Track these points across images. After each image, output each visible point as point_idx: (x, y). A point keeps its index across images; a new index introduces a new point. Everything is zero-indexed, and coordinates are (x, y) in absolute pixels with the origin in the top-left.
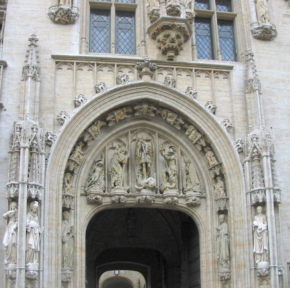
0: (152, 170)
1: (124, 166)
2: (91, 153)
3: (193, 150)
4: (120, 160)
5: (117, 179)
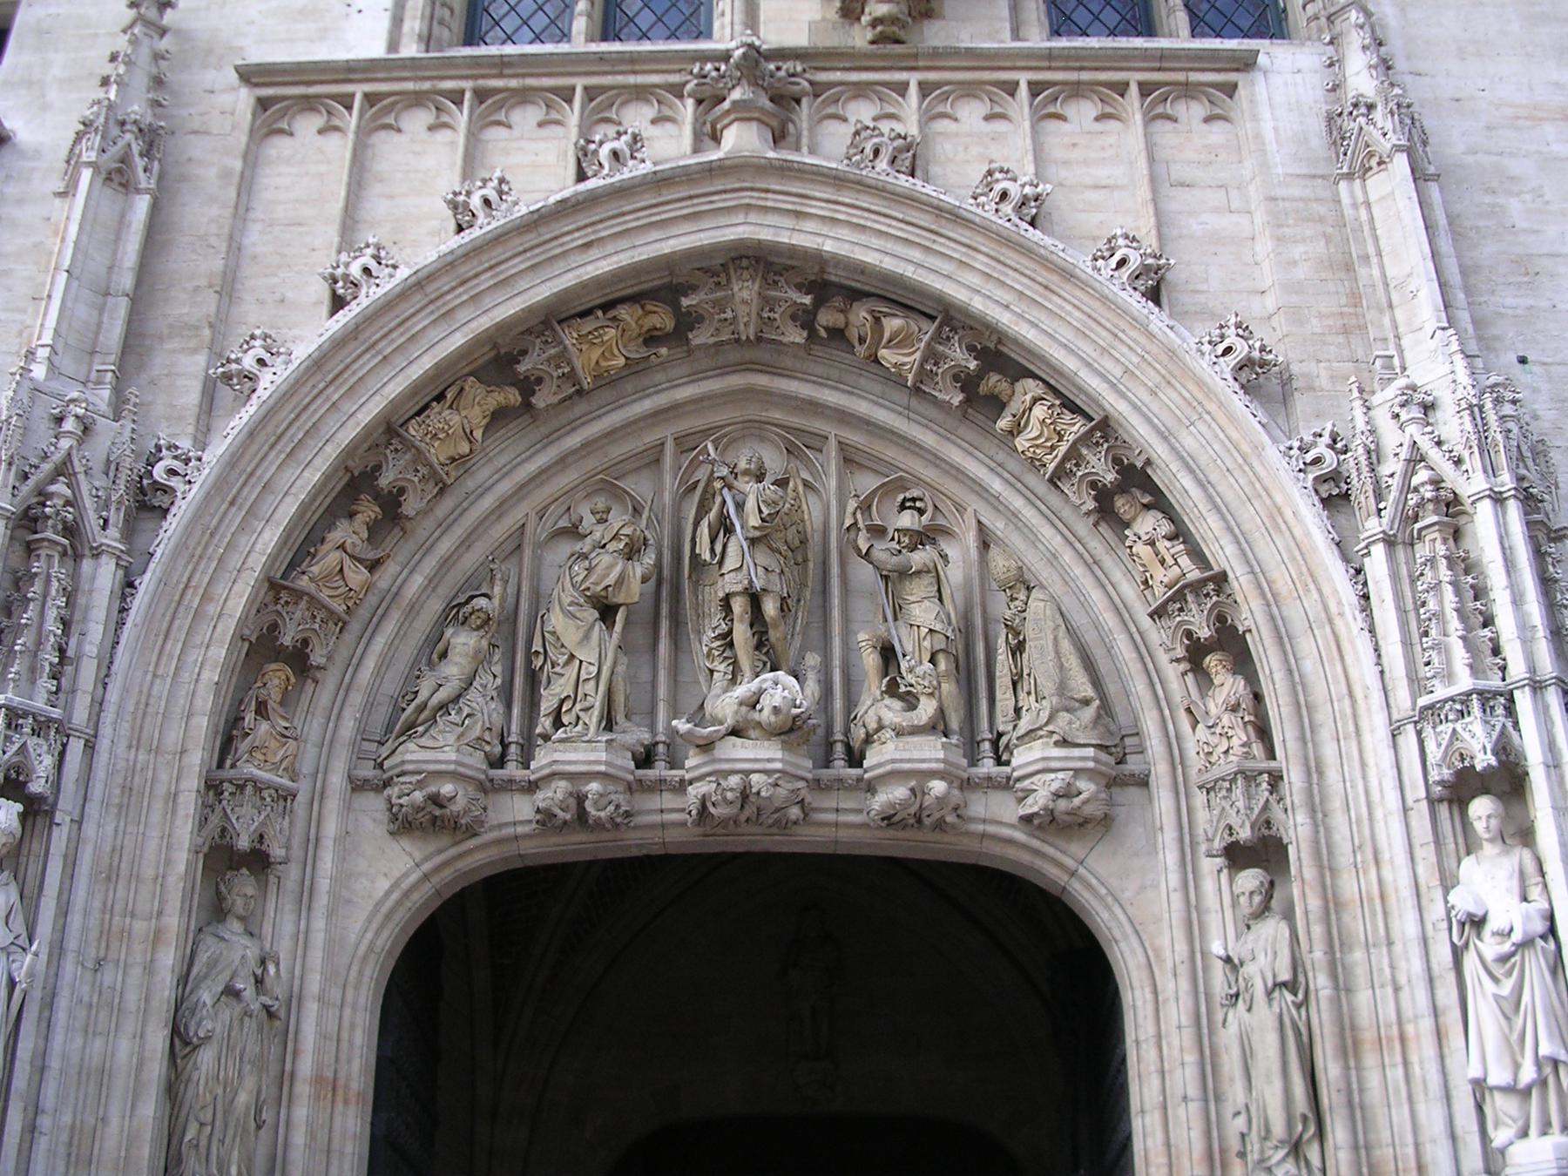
1: (620, 617)
2: (428, 558)
4: (596, 584)
5: (569, 691)
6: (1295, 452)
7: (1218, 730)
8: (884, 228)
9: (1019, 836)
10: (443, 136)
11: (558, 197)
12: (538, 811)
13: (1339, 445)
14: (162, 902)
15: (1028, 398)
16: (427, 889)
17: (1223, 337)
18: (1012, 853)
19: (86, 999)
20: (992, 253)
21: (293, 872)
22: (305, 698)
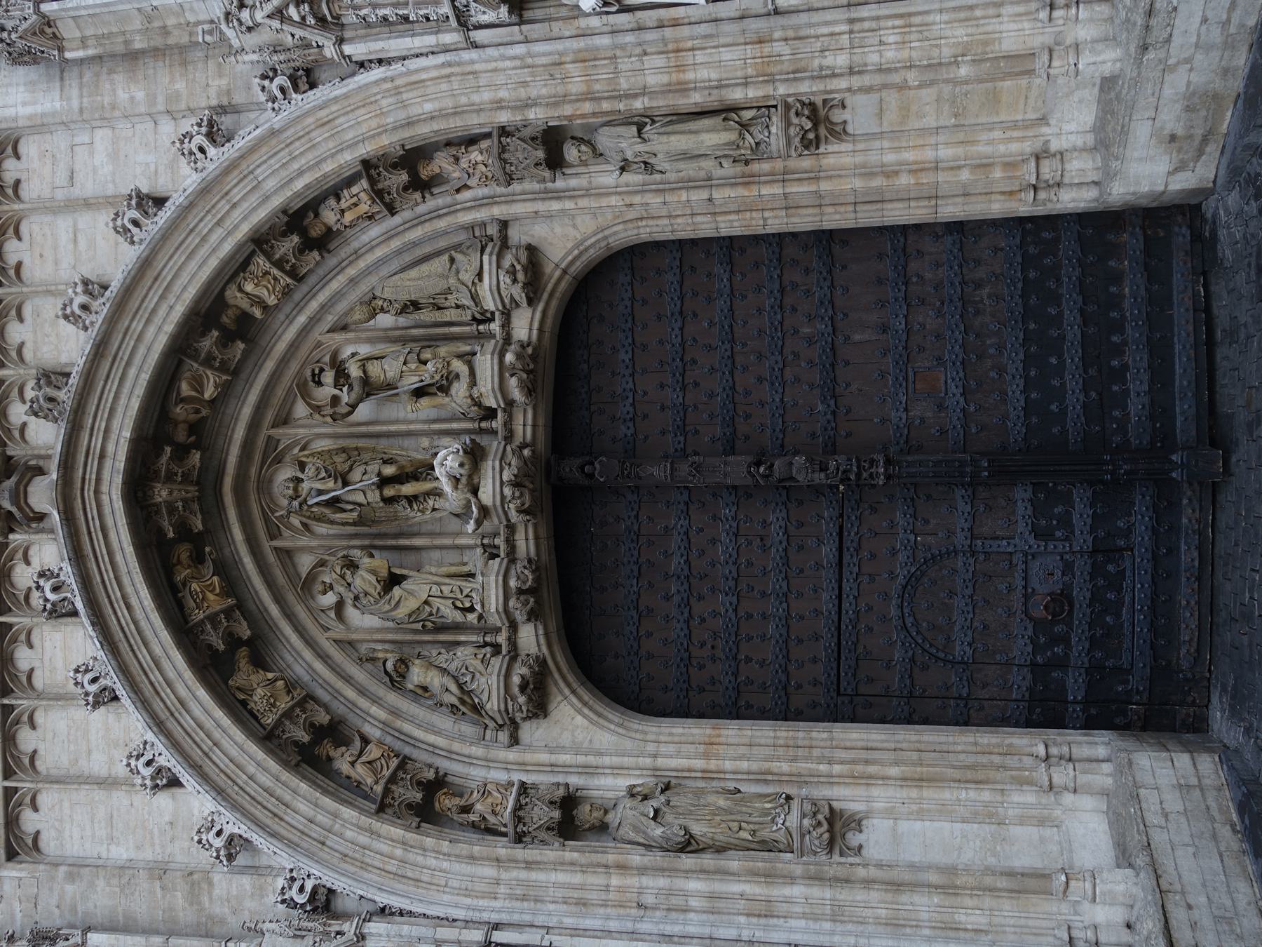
0: (414, 451)
1: (398, 571)
3: (324, 282)
5: (449, 602)
6: (276, 105)
7: (471, 171)
8: (112, 395)
9: (540, 307)
10: (39, 718)
11: (90, 629)
12: (529, 620)
13: (271, 74)
14: (599, 865)
15: (239, 295)
16: (581, 691)
17: (191, 153)
18: (551, 312)
19: (664, 913)
20: (130, 317)
21: (574, 780)
22: (458, 781)
